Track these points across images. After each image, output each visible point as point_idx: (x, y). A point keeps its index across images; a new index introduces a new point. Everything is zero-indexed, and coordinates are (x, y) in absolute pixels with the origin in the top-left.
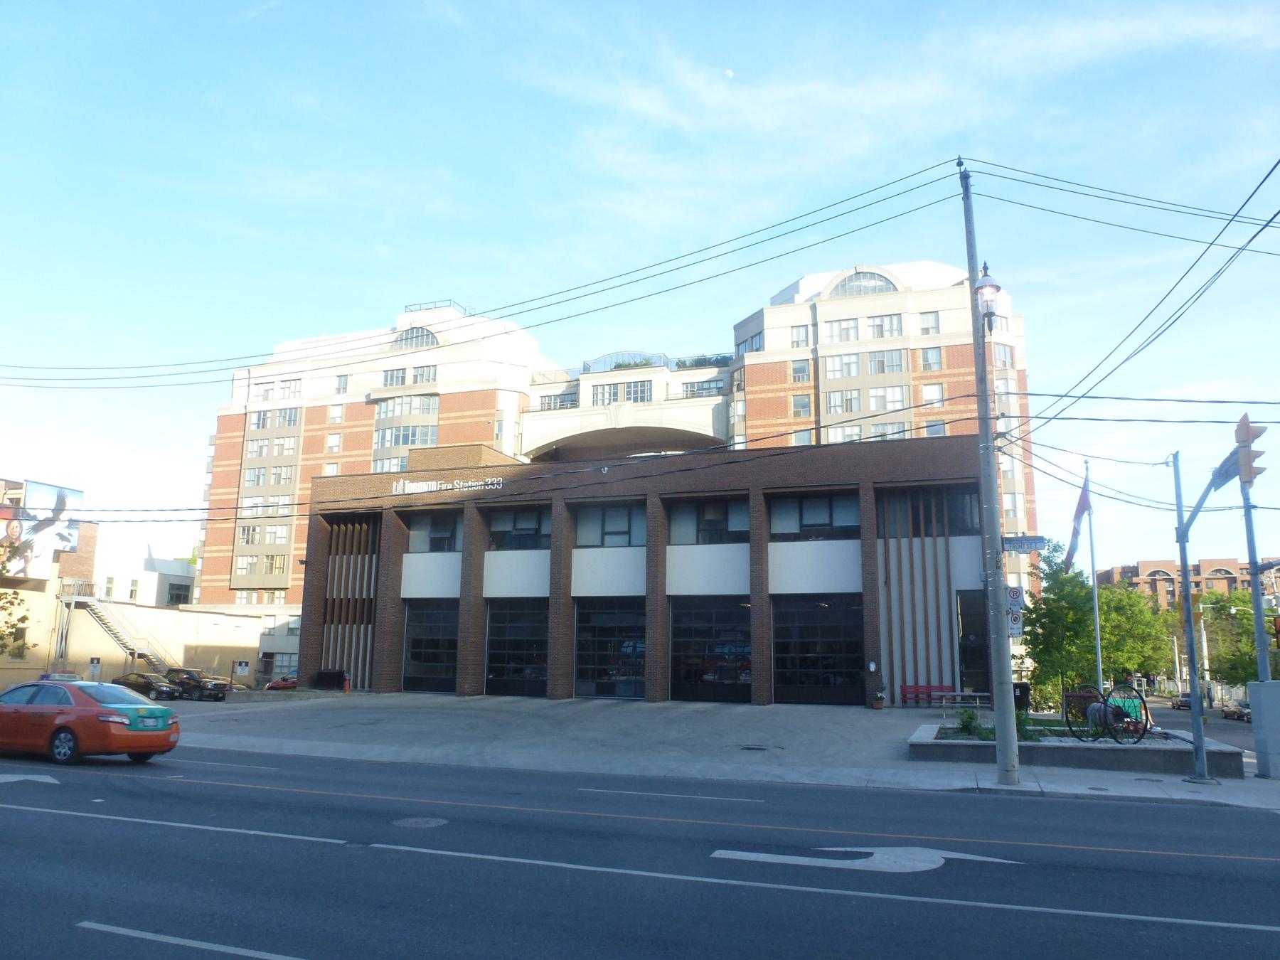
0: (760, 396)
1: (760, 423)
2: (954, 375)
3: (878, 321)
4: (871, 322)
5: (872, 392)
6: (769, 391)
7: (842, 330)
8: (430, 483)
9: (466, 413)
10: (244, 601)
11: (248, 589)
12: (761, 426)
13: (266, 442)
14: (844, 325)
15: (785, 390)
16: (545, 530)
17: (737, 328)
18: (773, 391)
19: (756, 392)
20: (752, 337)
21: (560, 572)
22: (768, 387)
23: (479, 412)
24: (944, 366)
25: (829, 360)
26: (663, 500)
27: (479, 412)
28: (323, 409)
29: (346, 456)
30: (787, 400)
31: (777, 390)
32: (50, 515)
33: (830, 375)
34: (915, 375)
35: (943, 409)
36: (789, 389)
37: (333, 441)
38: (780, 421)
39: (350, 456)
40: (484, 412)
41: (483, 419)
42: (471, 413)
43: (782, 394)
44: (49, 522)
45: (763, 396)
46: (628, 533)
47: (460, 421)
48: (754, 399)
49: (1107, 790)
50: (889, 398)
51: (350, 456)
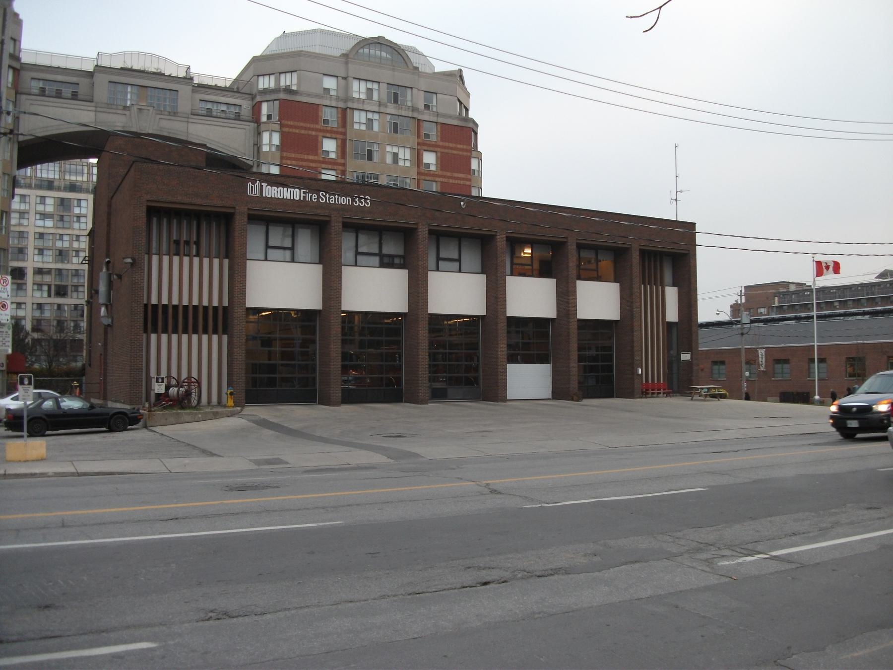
0: (294, 130)
1: (293, 155)
2: (445, 147)
5: (389, 149)
6: (302, 128)
8: (292, 190)
14: (370, 85)
15: (317, 130)
17: (255, 60)
18: (305, 129)
19: (291, 127)
20: (280, 73)
24: (439, 139)
25: (356, 113)
30: (318, 140)
31: (309, 129)
33: (356, 126)
34: (420, 140)
35: (437, 173)
36: (320, 131)
38: (311, 157)
43: (314, 133)
45: (297, 131)
46: (459, 260)
48: (289, 132)
50: (401, 156)
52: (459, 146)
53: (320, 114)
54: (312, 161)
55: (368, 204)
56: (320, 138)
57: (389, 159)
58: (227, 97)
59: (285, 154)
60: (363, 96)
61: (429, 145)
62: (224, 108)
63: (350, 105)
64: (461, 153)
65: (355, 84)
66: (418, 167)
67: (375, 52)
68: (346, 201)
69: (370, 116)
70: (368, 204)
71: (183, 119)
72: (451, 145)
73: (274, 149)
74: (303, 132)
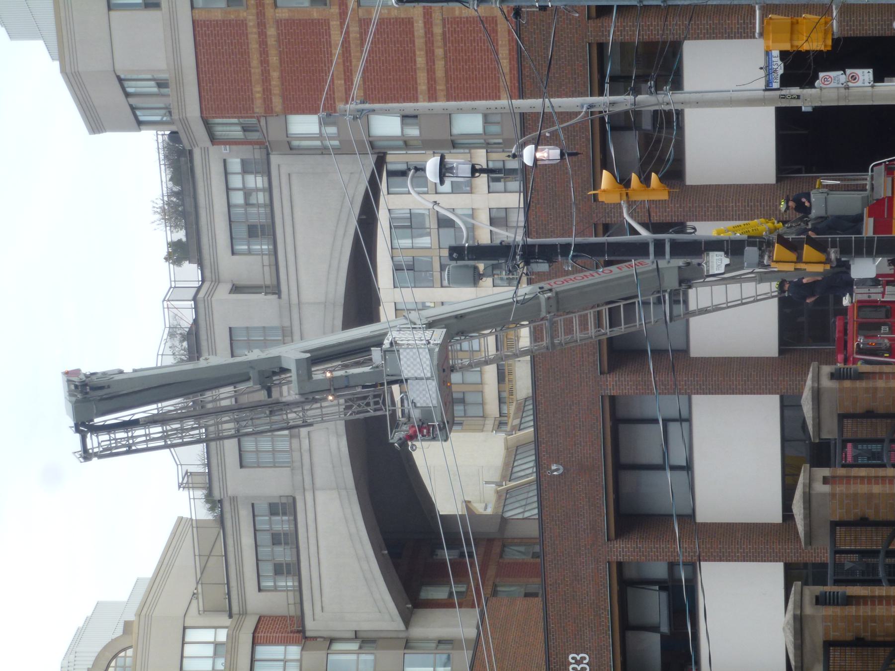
6: (264, 62)
15: (261, 25)
16: (659, 570)
22: (255, 62)
31: (263, 43)
36: (261, 14)
43: (272, 31)
45: (275, 75)
53: (219, 16)
55: (583, 658)
56: (282, 14)
58: (209, 194)
62: (238, 198)
70: (583, 658)
71: (295, 316)
73: (332, 130)
74: (274, 59)
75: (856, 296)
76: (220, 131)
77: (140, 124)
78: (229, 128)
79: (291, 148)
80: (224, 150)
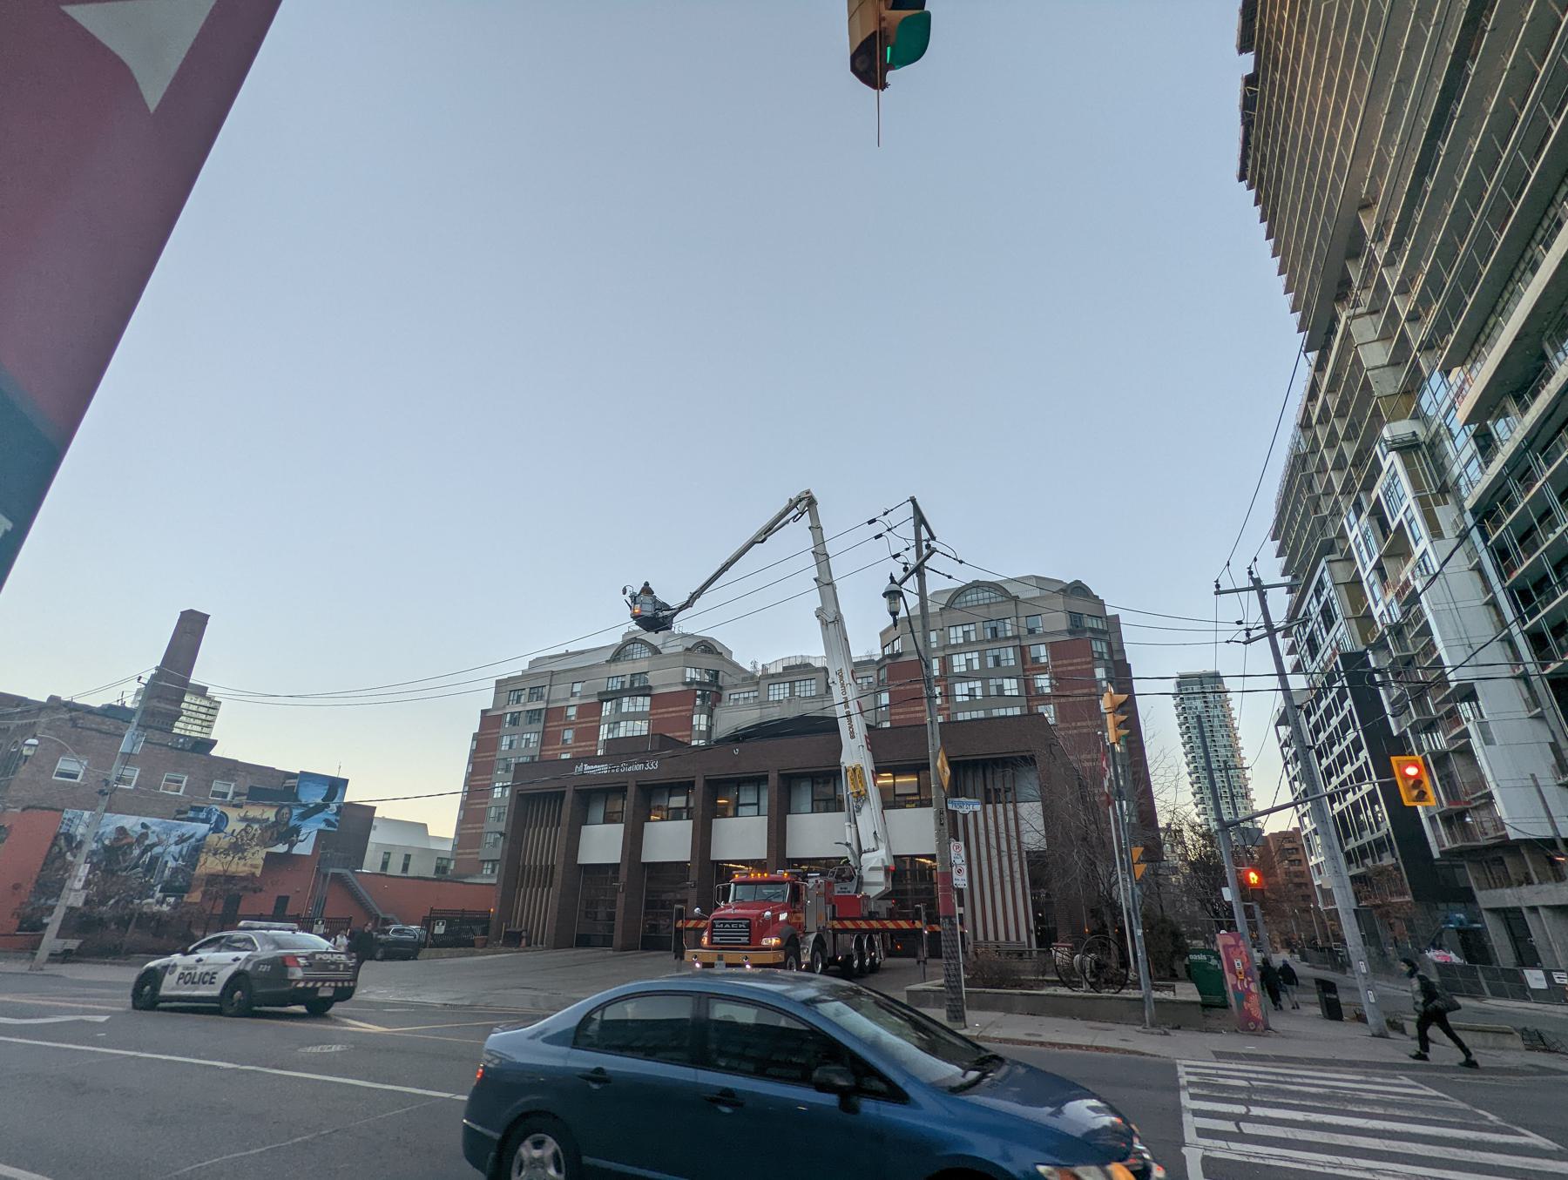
1: (901, 710)
3: (993, 624)
4: (987, 624)
5: (992, 682)
7: (964, 632)
9: (671, 709)
10: (489, 872)
11: (492, 861)
12: (902, 714)
13: (516, 737)
14: (966, 628)
17: (882, 634)
21: (703, 839)
23: (681, 708)
25: (955, 658)
26: (780, 775)
27: (681, 708)
28: (562, 710)
29: (576, 747)
32: (319, 800)
33: (956, 670)
37: (569, 735)
38: (917, 709)
39: (580, 747)
40: (684, 708)
41: (684, 714)
42: (674, 709)
44: (319, 809)
46: (758, 804)
47: (666, 716)
49: (1040, 1036)
51: (580, 747)
52: (1075, 661)
54: (918, 712)
57: (993, 691)
59: (893, 711)
60: (961, 641)
61: (1039, 669)
63: (948, 652)
64: (1079, 667)
65: (952, 630)
66: (1028, 692)
67: (984, 596)
68: (638, 767)
69: (969, 656)
72: (1065, 662)
75: (556, 701)
76: (882, 672)
77: (883, 648)
78: (883, 673)
79: (877, 693)
80: (875, 676)
